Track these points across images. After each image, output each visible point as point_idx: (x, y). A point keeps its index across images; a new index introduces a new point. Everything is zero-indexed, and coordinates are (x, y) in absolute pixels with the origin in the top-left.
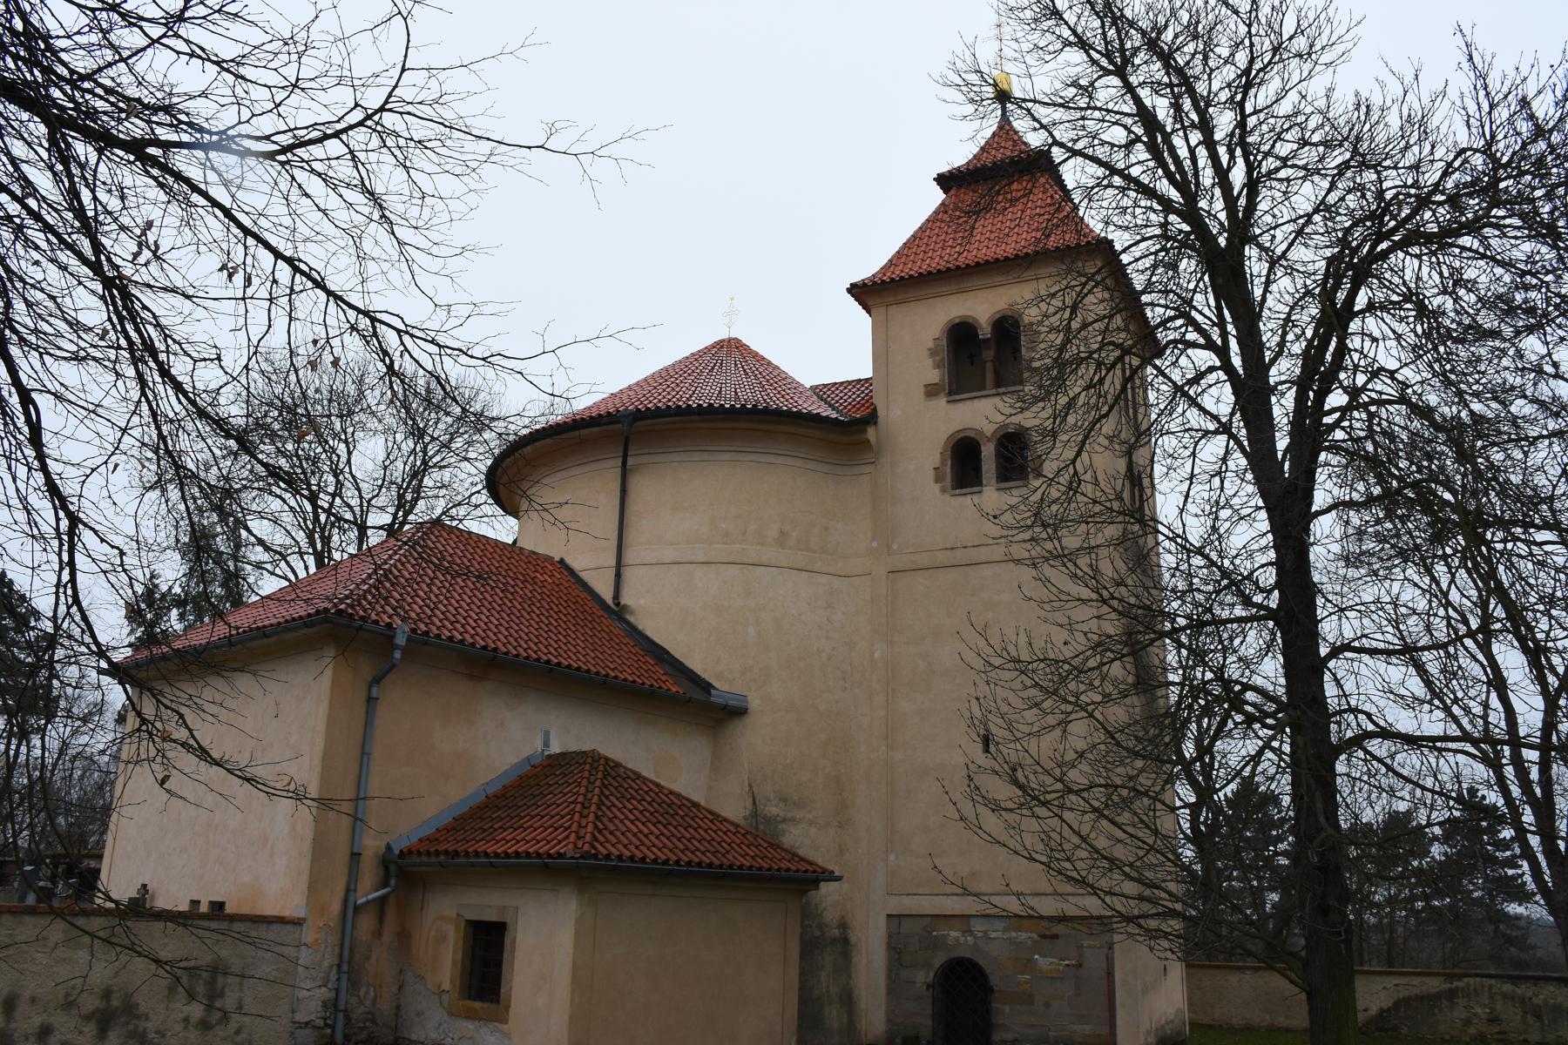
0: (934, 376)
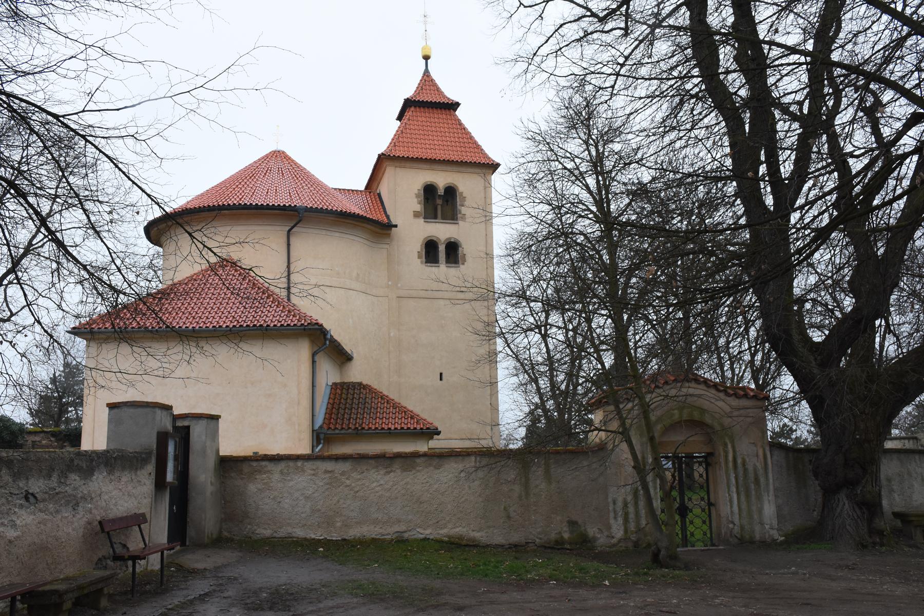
0: (418, 208)
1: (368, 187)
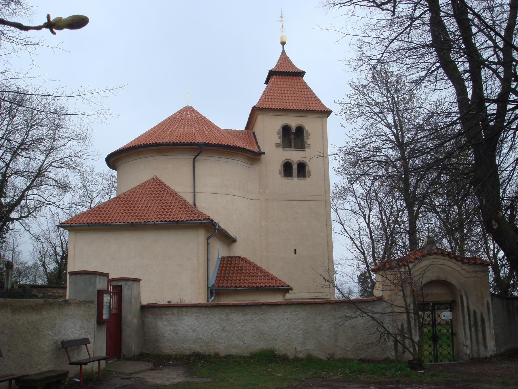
0: (279, 141)
1: (247, 128)
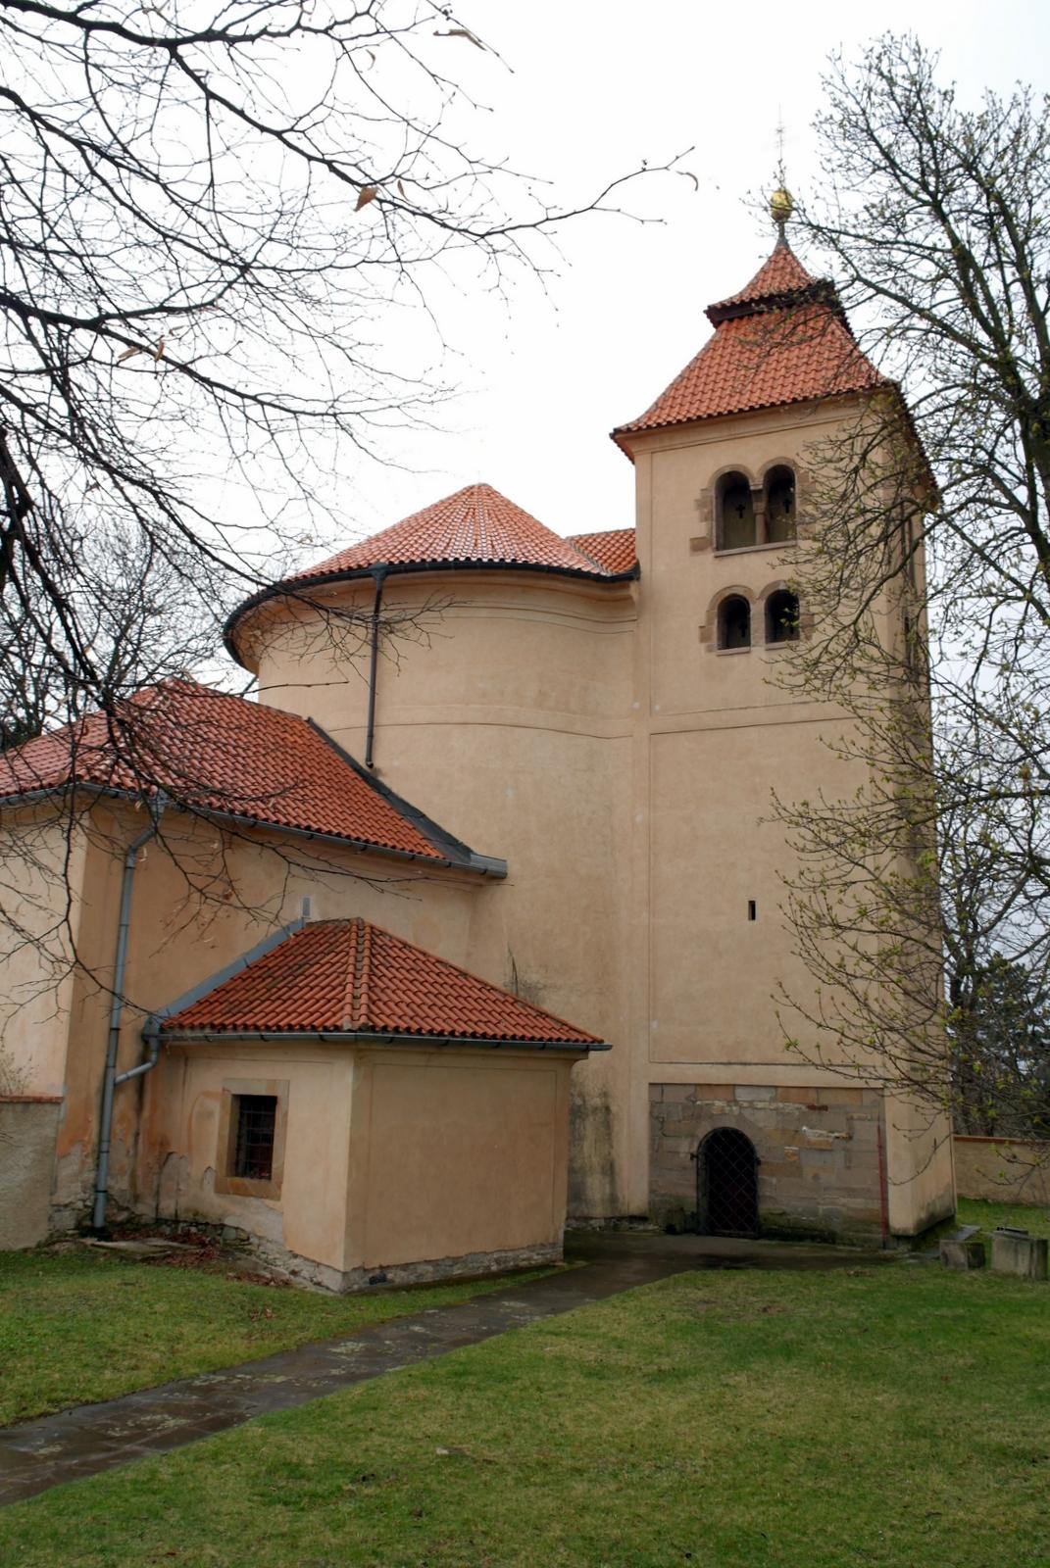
0: (702, 529)
